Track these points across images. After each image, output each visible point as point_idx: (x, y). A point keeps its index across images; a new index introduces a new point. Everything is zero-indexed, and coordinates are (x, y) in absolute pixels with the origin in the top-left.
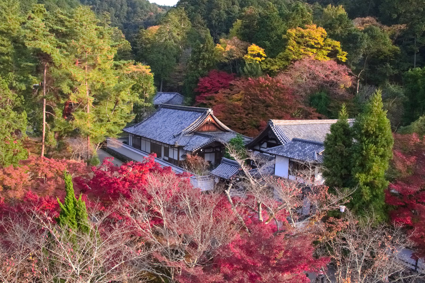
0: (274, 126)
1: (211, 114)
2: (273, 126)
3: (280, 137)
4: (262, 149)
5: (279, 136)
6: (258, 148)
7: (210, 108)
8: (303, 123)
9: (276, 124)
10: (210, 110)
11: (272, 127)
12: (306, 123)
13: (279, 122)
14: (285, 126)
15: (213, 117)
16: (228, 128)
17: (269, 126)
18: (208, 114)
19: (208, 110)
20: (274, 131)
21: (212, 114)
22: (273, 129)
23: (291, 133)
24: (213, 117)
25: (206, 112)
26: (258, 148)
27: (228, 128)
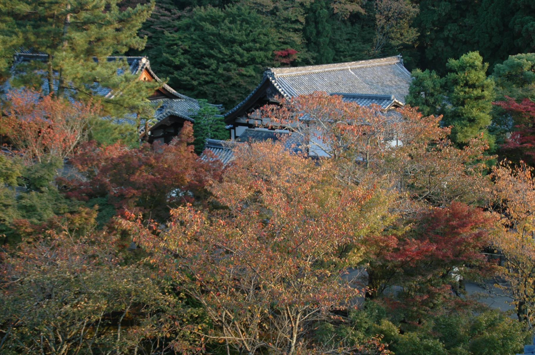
0: (276, 79)
1: (146, 69)
2: (274, 79)
3: (289, 95)
4: (251, 122)
5: (287, 96)
6: (244, 120)
7: (144, 56)
8: (317, 71)
9: (278, 75)
10: (144, 60)
11: (273, 81)
12: (320, 71)
13: (281, 72)
14: (292, 78)
15: (150, 73)
16: (173, 91)
17: (268, 79)
18: (143, 67)
19: (141, 59)
20: (277, 87)
21: (148, 67)
22: (275, 84)
23: (302, 88)
24: (150, 73)
25: (137, 65)
26: (244, 120)
27: (173, 91)
